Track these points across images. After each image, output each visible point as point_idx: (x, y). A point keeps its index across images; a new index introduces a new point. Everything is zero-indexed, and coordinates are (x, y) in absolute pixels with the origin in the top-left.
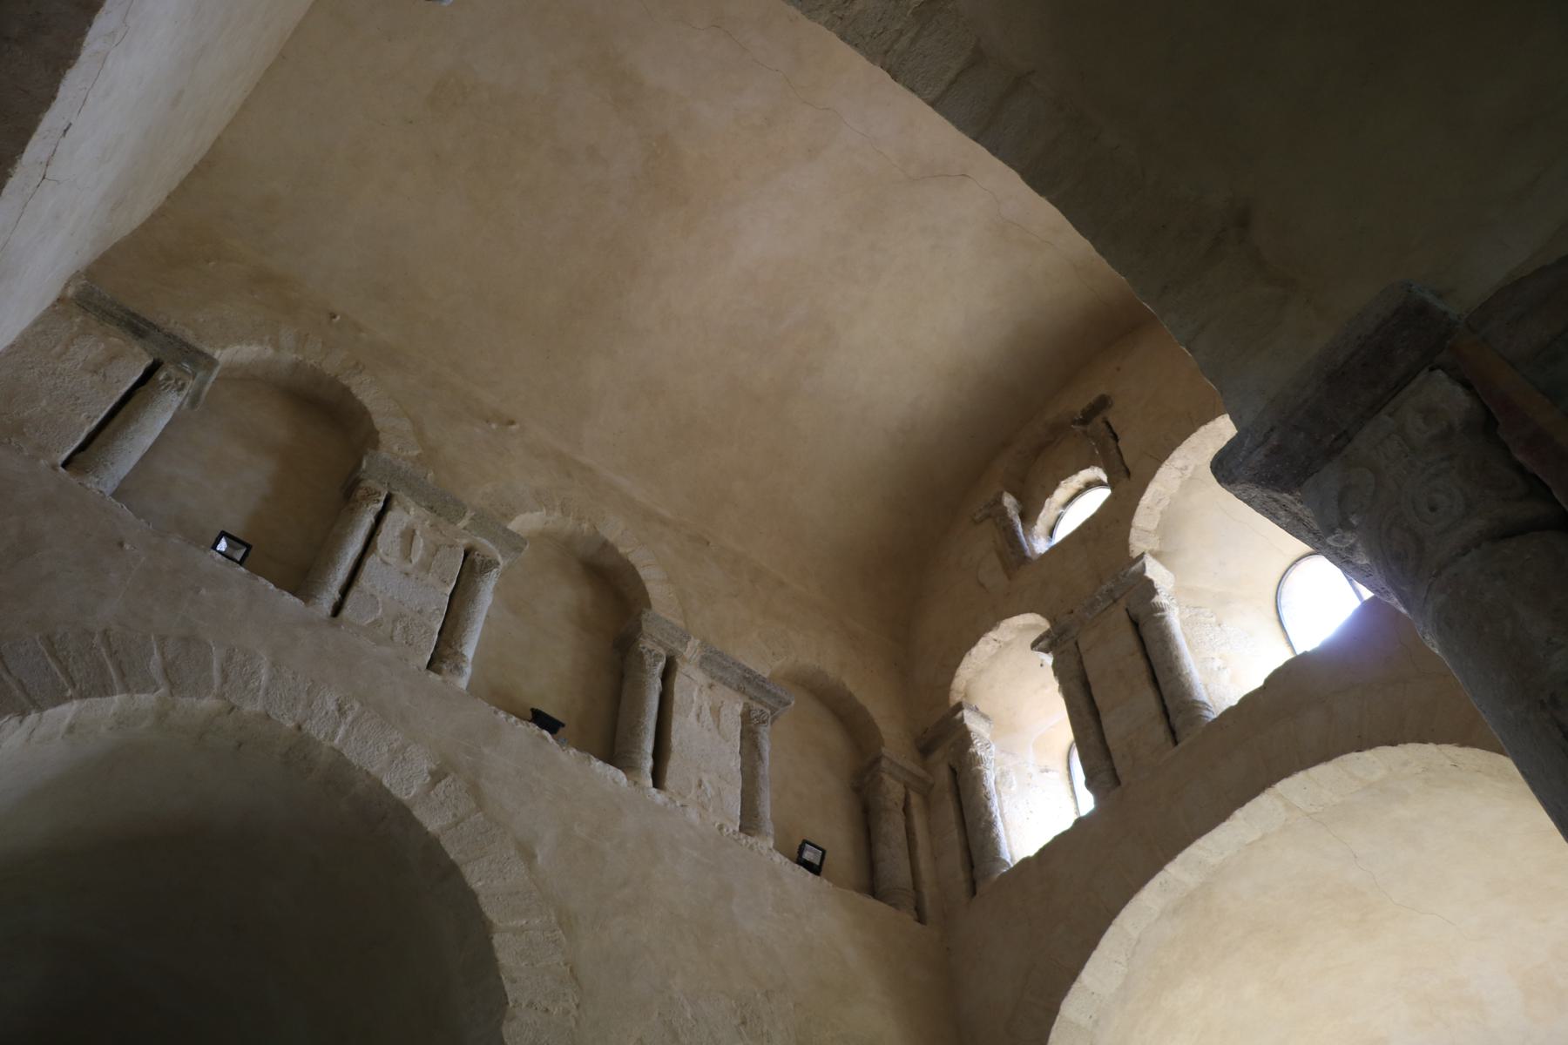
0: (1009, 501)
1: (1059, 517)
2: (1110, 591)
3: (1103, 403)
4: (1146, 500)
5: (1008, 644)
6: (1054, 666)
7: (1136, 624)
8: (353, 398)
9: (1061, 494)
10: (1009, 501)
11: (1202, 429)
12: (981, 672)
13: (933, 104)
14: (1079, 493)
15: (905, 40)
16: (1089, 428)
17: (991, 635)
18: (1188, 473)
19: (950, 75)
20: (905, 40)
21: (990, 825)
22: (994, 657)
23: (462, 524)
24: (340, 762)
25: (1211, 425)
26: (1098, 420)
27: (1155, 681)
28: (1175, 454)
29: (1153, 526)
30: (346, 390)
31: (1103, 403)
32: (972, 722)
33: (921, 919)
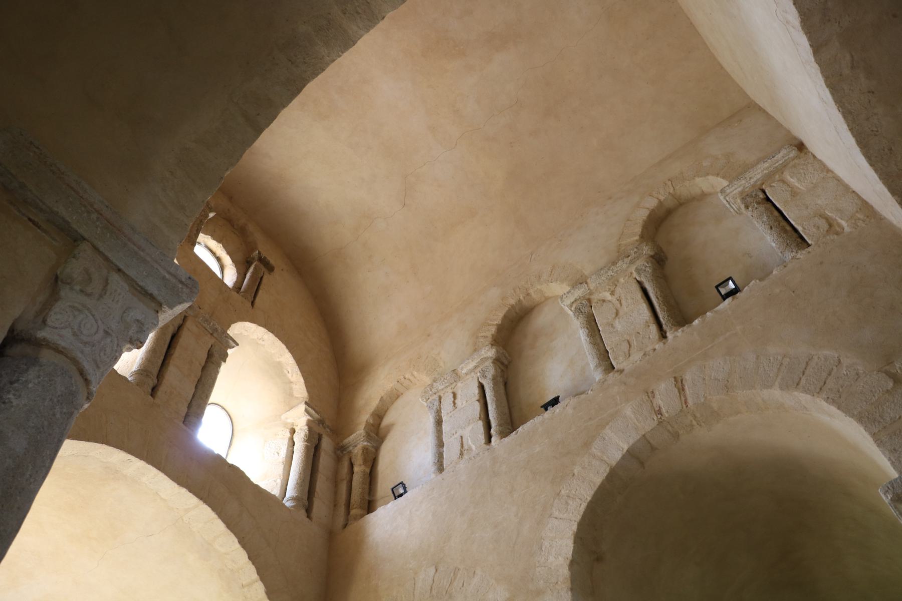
0: (211, 215)
2: (216, 330)
10: (211, 215)
13: (644, 436)
18: (260, 342)
19: (651, 441)
25: (287, 351)
26: (264, 269)
28: (271, 334)
31: (270, 269)
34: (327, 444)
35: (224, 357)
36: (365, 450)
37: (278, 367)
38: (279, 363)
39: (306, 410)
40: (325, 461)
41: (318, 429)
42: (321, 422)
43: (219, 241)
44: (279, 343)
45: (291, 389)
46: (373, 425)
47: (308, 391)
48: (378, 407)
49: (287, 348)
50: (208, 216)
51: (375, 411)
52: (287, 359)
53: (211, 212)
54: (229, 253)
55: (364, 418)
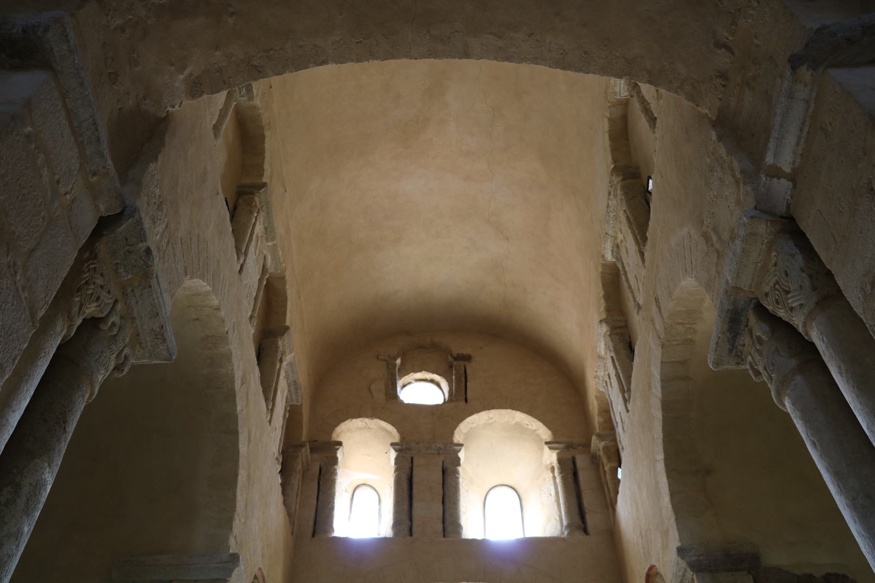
0: (398, 361)
1: (410, 383)
2: (440, 448)
3: (468, 358)
4: (469, 419)
5: (369, 428)
6: (397, 459)
7: (444, 472)
8: (263, 142)
9: (419, 375)
10: (398, 361)
11: (509, 410)
12: (349, 430)
13: (662, 362)
14: (425, 380)
15: (675, 343)
16: (455, 363)
17: (367, 420)
18: (491, 421)
19: (673, 360)
20: (675, 343)
21: (332, 509)
22: (361, 429)
23: (270, 244)
24: (228, 357)
25: (514, 412)
26: (462, 363)
27: (443, 502)
28: (493, 411)
29: (465, 431)
30: (263, 137)
31: (468, 358)
32: (339, 454)
33: (292, 533)
34: (582, 462)
35: (457, 462)
36: (606, 449)
37: (518, 426)
38: (517, 424)
39: (550, 448)
40: (584, 477)
41: (568, 455)
42: (569, 446)
43: (420, 371)
44: (503, 411)
45: (538, 435)
46: (605, 422)
47: (550, 429)
48: (599, 405)
49: (513, 409)
50: (395, 365)
51: (599, 410)
52: (519, 417)
53: (396, 360)
54: (433, 372)
55: (597, 420)
